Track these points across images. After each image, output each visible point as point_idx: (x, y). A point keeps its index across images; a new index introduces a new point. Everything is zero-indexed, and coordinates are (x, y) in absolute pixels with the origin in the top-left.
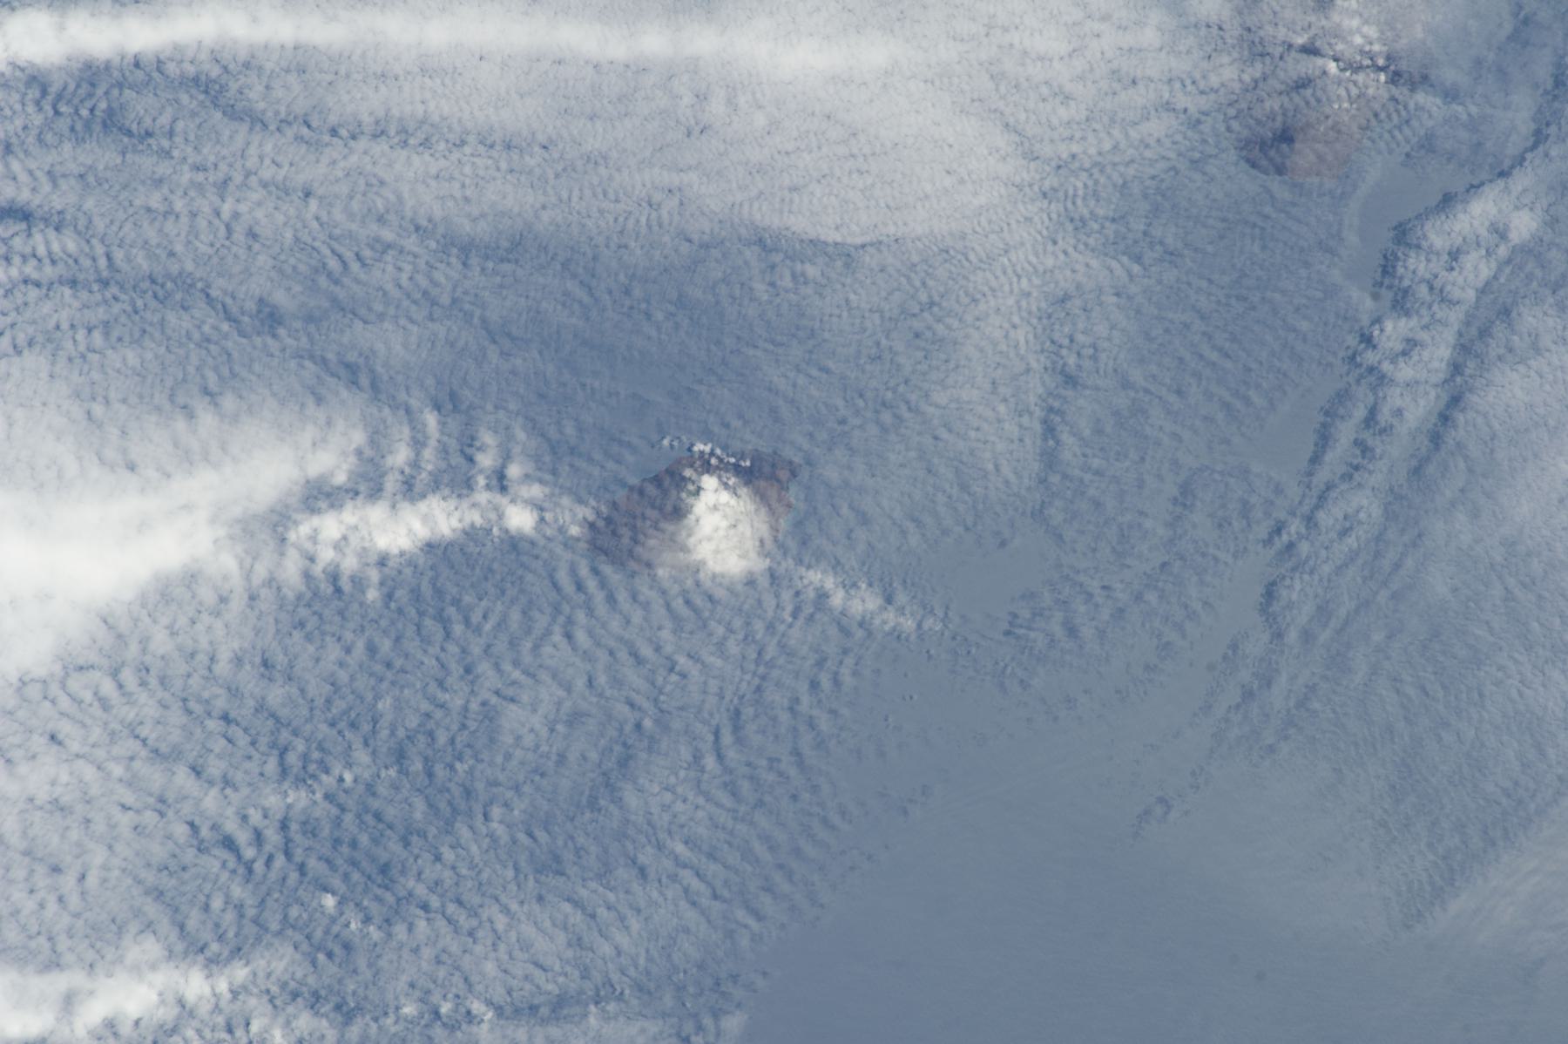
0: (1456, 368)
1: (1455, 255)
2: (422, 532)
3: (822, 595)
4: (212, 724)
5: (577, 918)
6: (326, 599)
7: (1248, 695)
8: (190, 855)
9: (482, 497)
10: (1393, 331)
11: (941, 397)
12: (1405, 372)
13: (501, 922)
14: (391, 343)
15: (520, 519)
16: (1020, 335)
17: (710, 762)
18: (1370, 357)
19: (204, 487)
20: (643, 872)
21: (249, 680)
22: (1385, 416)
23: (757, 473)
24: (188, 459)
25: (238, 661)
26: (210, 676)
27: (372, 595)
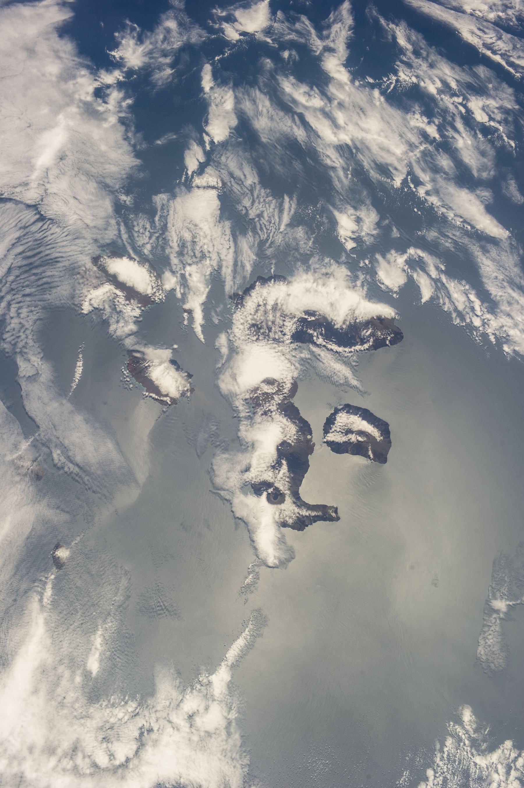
0: (73, 464)
1: (59, 460)
2: (50, 589)
3: (75, 543)
4: (66, 621)
5: (106, 584)
6: (54, 603)
7: (106, 498)
8: (82, 629)
9: (48, 581)
10: (66, 469)
11: (55, 522)
12: (72, 469)
13: (104, 593)
15: (53, 577)
16: (51, 511)
17: (92, 562)
18: (69, 473)
20: (104, 574)
21: (61, 615)
22: (76, 473)
23: (57, 547)
25: (59, 616)
26: (59, 620)
27: (56, 598)
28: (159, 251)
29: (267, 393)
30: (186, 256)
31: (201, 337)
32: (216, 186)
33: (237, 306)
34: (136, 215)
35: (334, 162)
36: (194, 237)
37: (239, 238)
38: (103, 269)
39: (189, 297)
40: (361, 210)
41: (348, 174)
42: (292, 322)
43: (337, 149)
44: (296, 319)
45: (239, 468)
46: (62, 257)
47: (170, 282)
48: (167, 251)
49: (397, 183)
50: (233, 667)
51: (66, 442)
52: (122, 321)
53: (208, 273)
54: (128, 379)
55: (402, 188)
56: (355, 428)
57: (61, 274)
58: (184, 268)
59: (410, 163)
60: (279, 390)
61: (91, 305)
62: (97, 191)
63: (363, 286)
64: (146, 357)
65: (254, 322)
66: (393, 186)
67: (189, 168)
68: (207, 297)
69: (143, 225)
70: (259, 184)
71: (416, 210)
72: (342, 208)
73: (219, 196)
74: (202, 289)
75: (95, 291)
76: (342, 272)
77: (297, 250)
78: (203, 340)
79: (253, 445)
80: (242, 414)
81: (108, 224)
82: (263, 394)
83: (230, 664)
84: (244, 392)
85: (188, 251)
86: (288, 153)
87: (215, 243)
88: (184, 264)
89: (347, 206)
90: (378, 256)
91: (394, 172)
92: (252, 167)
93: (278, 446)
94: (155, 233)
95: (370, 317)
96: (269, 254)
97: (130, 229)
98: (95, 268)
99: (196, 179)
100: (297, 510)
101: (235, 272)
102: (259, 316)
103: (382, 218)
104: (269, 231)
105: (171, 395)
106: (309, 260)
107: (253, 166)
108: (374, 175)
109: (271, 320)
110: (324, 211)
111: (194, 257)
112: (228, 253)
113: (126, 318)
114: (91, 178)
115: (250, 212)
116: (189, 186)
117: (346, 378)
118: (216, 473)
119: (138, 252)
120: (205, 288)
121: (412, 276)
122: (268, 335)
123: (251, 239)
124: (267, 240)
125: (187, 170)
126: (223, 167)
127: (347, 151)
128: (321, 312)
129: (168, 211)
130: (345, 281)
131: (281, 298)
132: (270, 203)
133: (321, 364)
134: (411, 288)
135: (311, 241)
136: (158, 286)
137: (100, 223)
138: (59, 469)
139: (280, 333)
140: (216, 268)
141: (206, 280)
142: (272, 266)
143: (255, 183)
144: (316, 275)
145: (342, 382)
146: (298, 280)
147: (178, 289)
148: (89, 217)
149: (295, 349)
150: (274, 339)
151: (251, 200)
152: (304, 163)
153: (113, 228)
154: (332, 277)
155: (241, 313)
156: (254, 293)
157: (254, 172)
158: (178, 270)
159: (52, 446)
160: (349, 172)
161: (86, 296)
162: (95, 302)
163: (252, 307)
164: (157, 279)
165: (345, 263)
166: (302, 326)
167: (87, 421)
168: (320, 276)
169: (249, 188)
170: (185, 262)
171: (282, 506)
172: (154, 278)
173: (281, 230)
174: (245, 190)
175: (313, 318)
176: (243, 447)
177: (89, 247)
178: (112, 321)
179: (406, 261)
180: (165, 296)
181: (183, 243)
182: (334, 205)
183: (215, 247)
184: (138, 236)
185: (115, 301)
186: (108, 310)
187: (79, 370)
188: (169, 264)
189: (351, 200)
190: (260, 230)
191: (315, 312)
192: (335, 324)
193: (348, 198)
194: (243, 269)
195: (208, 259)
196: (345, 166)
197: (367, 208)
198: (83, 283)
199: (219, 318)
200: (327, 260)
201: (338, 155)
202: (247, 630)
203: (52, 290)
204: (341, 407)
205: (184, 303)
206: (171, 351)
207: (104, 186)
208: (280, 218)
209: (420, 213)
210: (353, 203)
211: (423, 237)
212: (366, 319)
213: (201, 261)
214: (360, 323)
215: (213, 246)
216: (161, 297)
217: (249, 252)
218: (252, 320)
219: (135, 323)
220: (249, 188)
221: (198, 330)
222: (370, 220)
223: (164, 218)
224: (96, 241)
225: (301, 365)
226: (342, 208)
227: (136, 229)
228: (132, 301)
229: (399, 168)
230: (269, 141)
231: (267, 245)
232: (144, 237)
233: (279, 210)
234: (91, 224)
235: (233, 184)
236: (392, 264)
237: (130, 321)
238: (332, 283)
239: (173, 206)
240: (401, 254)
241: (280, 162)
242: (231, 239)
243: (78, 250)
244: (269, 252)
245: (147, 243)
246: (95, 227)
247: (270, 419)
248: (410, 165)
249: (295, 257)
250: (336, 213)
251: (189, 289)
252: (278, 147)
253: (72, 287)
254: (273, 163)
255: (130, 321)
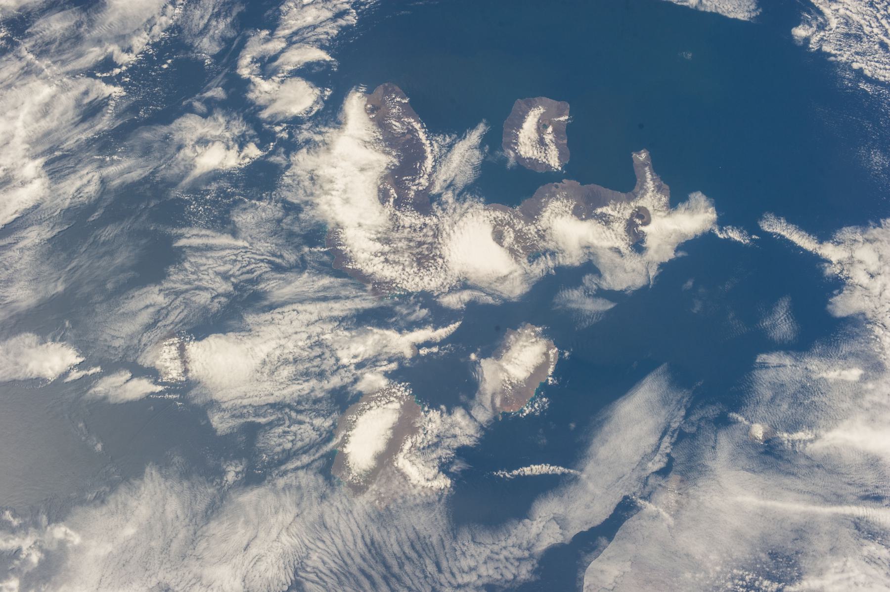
0: (660, 444)
6: (810, 426)
10: (668, 451)
12: (667, 444)
14: (802, 461)
15: (785, 435)
19: (826, 444)
21: (819, 415)
24: (828, 448)
28: (323, 406)
29: (516, 239)
30: (323, 367)
31: (453, 327)
32: (178, 345)
33: (394, 289)
34: (261, 451)
35: (89, 182)
36: (286, 362)
37: (274, 300)
38: (371, 475)
39: (393, 351)
40: (181, 139)
41: (113, 160)
42: (402, 217)
43: (60, 178)
44: (397, 212)
45: (618, 260)
46: (363, 537)
47: (373, 380)
48: (319, 394)
49: (116, 91)
50: (821, 242)
51: (637, 458)
52: (452, 431)
53: (346, 333)
54: (536, 405)
55: (123, 84)
56: (535, 136)
57: (393, 530)
58: (344, 366)
59: (67, 73)
60: (508, 224)
61: (435, 477)
62: (225, 518)
63: (320, 133)
64: (499, 390)
65: (415, 265)
66: (121, 97)
67: (149, 391)
68: (387, 326)
69: (279, 437)
70: (162, 285)
71: (165, 66)
72: (184, 165)
73: (199, 338)
74: (377, 337)
75: (413, 478)
76: (303, 161)
77: (279, 221)
78: (457, 324)
79: (588, 247)
80: (551, 264)
81: (287, 487)
82: (518, 242)
83: (817, 246)
84: (520, 264)
85: (314, 367)
86: (84, 249)
87: (291, 330)
88: (338, 368)
89: (180, 158)
90: (265, 115)
91: (92, 96)
92: (127, 298)
93: (582, 220)
94: (290, 418)
95: (372, 123)
96: (295, 257)
97: (289, 455)
98: (374, 487)
99: (170, 377)
100: (650, 194)
101: (337, 298)
102: (405, 259)
103: (190, 110)
104: (253, 261)
105: (545, 350)
106: (293, 203)
107: (125, 296)
108: (104, 123)
109: (406, 243)
110: (194, 189)
111: (323, 357)
112: (306, 311)
113: (447, 427)
114: (199, 533)
115: (220, 290)
116: (186, 386)
117: (470, 148)
118: (630, 284)
119: (330, 435)
120: (374, 334)
121: (290, 72)
122: (431, 244)
123: (273, 284)
124: (269, 262)
125: (153, 393)
126: (136, 341)
127: (58, 163)
128: (379, 183)
129: (245, 407)
130: (318, 156)
131: (368, 235)
132: (198, 266)
133: (457, 178)
134: (306, 72)
135: (257, 203)
136: (383, 396)
137: (288, 500)
138: (671, 460)
139: (425, 230)
140: (336, 324)
141: (359, 334)
142: (316, 250)
143: (160, 291)
144: (318, 192)
145: (477, 153)
146: (333, 215)
147: (384, 368)
148: (280, 518)
149: (444, 210)
150: (435, 236)
151: (197, 292)
152: (103, 222)
153: (294, 478)
154: (315, 172)
155: (405, 282)
156: (369, 269)
157: (136, 293)
158: (350, 375)
159: (644, 474)
160: (108, 159)
161: (423, 487)
162: (429, 473)
163: (391, 269)
164: (375, 399)
165: (288, 157)
166: (407, 204)
167: (604, 442)
168: (317, 187)
169: (173, 297)
170: (335, 368)
171: (650, 209)
172: (373, 404)
173: (247, 245)
174: (177, 302)
175: (392, 191)
176: (592, 258)
177: (335, 504)
178: (456, 445)
179: (263, 79)
180: (400, 383)
181: (302, 375)
182: (182, 177)
183: (298, 330)
184: (302, 440)
185: (422, 447)
186: (440, 452)
187: (536, 469)
188: (344, 387)
189: (166, 154)
190: (253, 273)
191: (379, 190)
192: (394, 165)
193: (161, 158)
194: (329, 288)
195: (323, 337)
196: (95, 165)
197: (177, 131)
198: (402, 497)
199: (418, 308)
200: (287, 180)
201: (72, 176)
202: (782, 233)
203: (422, 536)
204: (511, 152)
205: (404, 358)
206: (482, 361)
207: (213, 510)
208: (223, 248)
209: (169, 61)
210: (172, 150)
211: (217, 58)
212: (375, 127)
213: (327, 346)
214: (383, 135)
215: (296, 333)
216: (403, 389)
217: (297, 283)
218: (412, 267)
219: (450, 412)
220: (173, 297)
221: (442, 333)
222: (199, 126)
223: (258, 410)
224: (323, 497)
225: (464, 201)
226: (184, 165)
227: (289, 445)
228: (418, 425)
229: (82, 88)
230: (61, 279)
231: (278, 261)
232: (302, 431)
233: (206, 250)
234: (295, 511)
235: (168, 322)
236: (274, 97)
237: (449, 421)
238: (325, 171)
239: (232, 402)
240: (254, 85)
241: (107, 258)
242: (277, 310)
243: (345, 518)
244: (291, 257)
245: (312, 425)
246: (298, 505)
247: (548, 231)
248: (73, 74)
249: (293, 223)
250: (197, 172)
251: (379, 355)
252: (73, 265)
253: (412, 509)
254: (111, 269)
255: (449, 421)
